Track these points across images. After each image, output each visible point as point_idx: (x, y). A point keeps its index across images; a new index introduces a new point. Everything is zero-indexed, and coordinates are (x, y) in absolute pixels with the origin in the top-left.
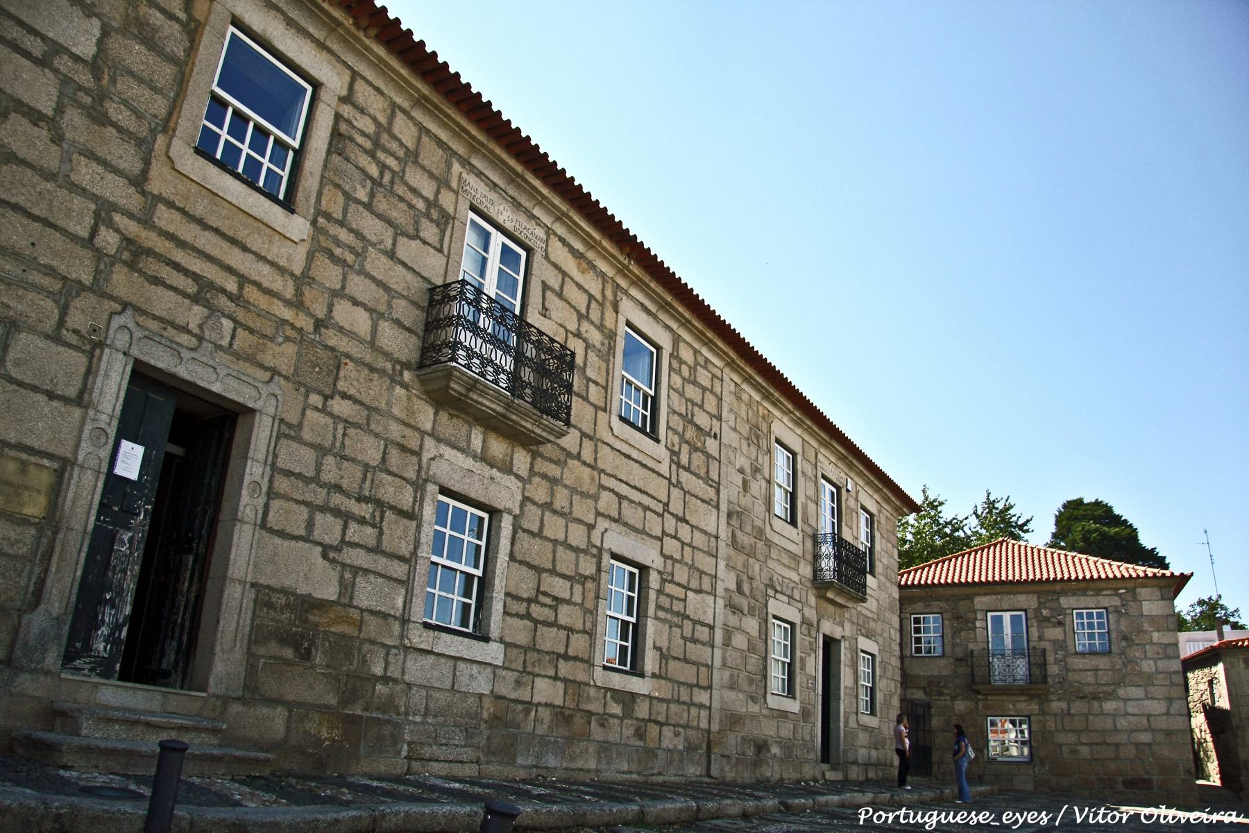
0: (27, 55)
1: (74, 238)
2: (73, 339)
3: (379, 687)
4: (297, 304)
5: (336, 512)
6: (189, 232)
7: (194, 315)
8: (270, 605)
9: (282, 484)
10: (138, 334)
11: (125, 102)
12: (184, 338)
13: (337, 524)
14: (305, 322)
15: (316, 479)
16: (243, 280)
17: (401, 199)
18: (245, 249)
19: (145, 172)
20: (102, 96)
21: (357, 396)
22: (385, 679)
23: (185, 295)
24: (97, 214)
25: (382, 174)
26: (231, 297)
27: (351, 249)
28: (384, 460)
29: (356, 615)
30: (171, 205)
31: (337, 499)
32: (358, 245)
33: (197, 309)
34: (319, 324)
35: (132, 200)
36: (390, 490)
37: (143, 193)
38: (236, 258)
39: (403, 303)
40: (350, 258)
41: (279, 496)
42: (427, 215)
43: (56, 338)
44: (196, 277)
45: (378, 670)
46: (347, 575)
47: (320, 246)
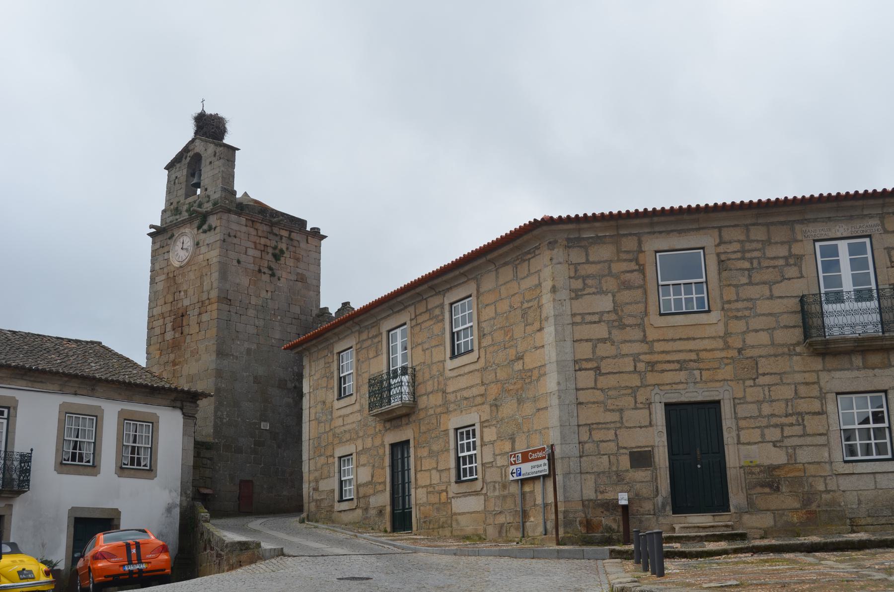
0: (595, 322)
1: (630, 372)
2: (641, 406)
3: (824, 496)
4: (727, 347)
5: (776, 426)
6: (668, 346)
7: (682, 376)
8: (752, 473)
9: (743, 423)
10: (662, 393)
11: (629, 316)
12: (681, 386)
13: (778, 431)
14: (734, 353)
15: (760, 416)
16: (697, 352)
17: (767, 267)
18: (694, 339)
19: (645, 336)
20: (620, 319)
21: (771, 371)
22: (827, 491)
23: (676, 370)
24: (634, 360)
25: (752, 263)
26: (695, 361)
27: (746, 309)
28: (796, 393)
29: (801, 466)
30: (659, 340)
31: (774, 420)
32: (749, 304)
33: (682, 373)
34: (740, 351)
35: (645, 348)
36: (803, 406)
37: (647, 343)
38: (691, 345)
39: (785, 316)
40: (747, 313)
41: (743, 429)
42: (787, 265)
43: (636, 408)
44: (678, 362)
45: (821, 487)
46: (790, 451)
47: (730, 316)
